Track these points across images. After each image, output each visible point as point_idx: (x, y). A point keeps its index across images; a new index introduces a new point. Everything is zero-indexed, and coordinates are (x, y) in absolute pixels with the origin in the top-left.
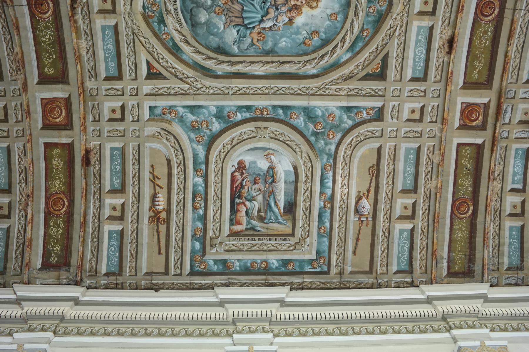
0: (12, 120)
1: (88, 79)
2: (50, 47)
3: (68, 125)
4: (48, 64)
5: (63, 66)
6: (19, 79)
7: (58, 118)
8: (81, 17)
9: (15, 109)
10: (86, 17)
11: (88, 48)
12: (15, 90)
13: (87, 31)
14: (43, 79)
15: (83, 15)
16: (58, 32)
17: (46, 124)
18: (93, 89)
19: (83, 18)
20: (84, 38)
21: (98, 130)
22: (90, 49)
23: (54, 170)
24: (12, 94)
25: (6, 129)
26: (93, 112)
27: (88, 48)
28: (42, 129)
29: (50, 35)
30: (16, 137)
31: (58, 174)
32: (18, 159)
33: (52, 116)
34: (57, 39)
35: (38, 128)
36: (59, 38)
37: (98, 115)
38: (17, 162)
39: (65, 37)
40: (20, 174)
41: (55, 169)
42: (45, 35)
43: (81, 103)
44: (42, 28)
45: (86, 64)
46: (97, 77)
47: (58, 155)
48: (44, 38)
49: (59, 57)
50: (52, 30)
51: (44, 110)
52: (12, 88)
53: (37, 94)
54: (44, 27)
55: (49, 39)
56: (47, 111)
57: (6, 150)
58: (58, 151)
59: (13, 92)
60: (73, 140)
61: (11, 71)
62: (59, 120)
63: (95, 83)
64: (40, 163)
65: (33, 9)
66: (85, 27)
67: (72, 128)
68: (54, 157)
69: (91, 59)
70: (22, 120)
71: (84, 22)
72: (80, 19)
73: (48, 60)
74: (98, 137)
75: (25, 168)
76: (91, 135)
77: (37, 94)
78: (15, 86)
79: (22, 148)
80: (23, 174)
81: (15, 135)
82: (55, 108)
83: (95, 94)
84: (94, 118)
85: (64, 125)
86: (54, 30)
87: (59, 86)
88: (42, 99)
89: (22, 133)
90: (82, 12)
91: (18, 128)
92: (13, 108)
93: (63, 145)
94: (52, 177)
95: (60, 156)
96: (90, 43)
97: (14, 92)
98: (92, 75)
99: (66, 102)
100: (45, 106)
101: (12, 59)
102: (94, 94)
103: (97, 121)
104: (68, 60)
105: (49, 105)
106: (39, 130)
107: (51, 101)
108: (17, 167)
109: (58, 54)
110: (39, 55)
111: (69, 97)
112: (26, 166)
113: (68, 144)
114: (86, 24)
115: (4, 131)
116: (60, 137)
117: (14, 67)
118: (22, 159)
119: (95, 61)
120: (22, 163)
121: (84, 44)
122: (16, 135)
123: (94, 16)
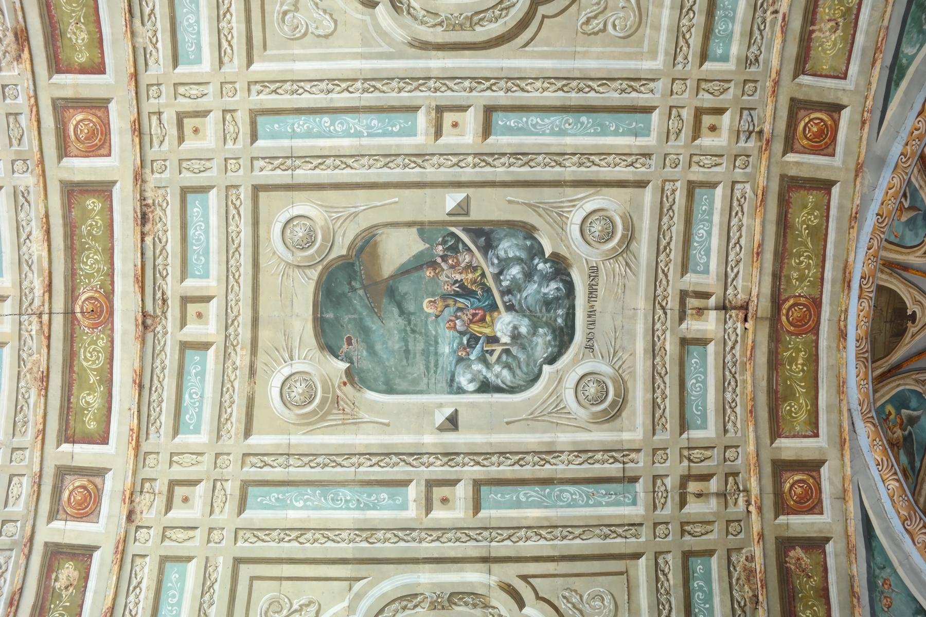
0: (169, 117)
1: (31, 189)
2: (89, 244)
3: (62, 107)
4: (95, 216)
5: (70, 212)
6: (152, 190)
7: (81, 121)
8: (36, 291)
9: (164, 137)
10: (27, 291)
11: (27, 241)
12: (160, 171)
13: (27, 268)
14: (106, 191)
15: (32, 295)
16: (72, 269)
17: (103, 109)
18: (21, 171)
19: (32, 290)
20: (35, 258)
21: (8, 99)
22: (25, 240)
23: (82, 20)
24: (167, 163)
25: (181, 100)
26: (21, 132)
27: (27, 241)
28: (108, 100)
29: (86, 264)
30: (161, 84)
31: (74, 11)
32: (157, 41)
33: (91, 125)
34: (76, 257)
35: (117, 102)
36: (72, 259)
37: (11, 126)
38: (159, 35)
39: (62, 261)
40: (153, 10)
41: (80, 21)
42: (94, 263)
43: (37, 148)
44: (98, 274)
45: (33, 214)
46: (15, 192)
47: (77, 51)
48: (96, 259)
49: (75, 227)
50: (83, 271)
51: (106, 135)
52: (166, 175)
53: (117, 164)
54: (94, 277)
55: (88, 258)
56: (102, 134)
57: (180, 59)
58: (78, 59)
59: (166, 167)
60: (50, 78)
61: (165, 205)
62: (79, 117)
63: (17, 183)
64: (112, 34)
65: (106, 304)
66: (30, 275)
67: (54, 101)
68: (84, 45)
69: (24, 223)
70: (149, 117)
71: (32, 283)
72: (37, 288)
73: (94, 223)
74: (8, 85)
75: (143, 24)
76: (19, 88)
77: (117, 164)
78: (161, 178)
79: (151, 62)
80: (147, 11)
81: (163, 88)
82: (86, 139)
83: (17, 163)
84: (16, 120)
85: (68, 108)
86: (78, 271)
87: (77, 178)
88: (109, 155)
89: (150, 92)
90: (33, 300)
91: (157, 101)
92: (167, 138)
93: (69, 71)
94: (84, 6)
95: (73, 47)
96: (24, 249)
97: (163, 167)
98: (23, 196)
99: (66, 149)
100: (105, 142)
101: (159, 225)
102: (19, 163)
103: (11, 114)
104: (60, 221)
105: (96, 145)
106: (115, 99)
107: (93, 151)
108: (159, 25)
109: (77, 232)
110: (109, 232)
111: (60, 158)
112: (141, 27)
113: (59, 71)
114: (28, 279)
115: (184, 96)
116: (76, 86)
117: (158, 212)
118: (151, 42)
119: (17, 220)
120: (150, 34)
121: (37, 248)
122: (161, 87)
123: (14, 292)
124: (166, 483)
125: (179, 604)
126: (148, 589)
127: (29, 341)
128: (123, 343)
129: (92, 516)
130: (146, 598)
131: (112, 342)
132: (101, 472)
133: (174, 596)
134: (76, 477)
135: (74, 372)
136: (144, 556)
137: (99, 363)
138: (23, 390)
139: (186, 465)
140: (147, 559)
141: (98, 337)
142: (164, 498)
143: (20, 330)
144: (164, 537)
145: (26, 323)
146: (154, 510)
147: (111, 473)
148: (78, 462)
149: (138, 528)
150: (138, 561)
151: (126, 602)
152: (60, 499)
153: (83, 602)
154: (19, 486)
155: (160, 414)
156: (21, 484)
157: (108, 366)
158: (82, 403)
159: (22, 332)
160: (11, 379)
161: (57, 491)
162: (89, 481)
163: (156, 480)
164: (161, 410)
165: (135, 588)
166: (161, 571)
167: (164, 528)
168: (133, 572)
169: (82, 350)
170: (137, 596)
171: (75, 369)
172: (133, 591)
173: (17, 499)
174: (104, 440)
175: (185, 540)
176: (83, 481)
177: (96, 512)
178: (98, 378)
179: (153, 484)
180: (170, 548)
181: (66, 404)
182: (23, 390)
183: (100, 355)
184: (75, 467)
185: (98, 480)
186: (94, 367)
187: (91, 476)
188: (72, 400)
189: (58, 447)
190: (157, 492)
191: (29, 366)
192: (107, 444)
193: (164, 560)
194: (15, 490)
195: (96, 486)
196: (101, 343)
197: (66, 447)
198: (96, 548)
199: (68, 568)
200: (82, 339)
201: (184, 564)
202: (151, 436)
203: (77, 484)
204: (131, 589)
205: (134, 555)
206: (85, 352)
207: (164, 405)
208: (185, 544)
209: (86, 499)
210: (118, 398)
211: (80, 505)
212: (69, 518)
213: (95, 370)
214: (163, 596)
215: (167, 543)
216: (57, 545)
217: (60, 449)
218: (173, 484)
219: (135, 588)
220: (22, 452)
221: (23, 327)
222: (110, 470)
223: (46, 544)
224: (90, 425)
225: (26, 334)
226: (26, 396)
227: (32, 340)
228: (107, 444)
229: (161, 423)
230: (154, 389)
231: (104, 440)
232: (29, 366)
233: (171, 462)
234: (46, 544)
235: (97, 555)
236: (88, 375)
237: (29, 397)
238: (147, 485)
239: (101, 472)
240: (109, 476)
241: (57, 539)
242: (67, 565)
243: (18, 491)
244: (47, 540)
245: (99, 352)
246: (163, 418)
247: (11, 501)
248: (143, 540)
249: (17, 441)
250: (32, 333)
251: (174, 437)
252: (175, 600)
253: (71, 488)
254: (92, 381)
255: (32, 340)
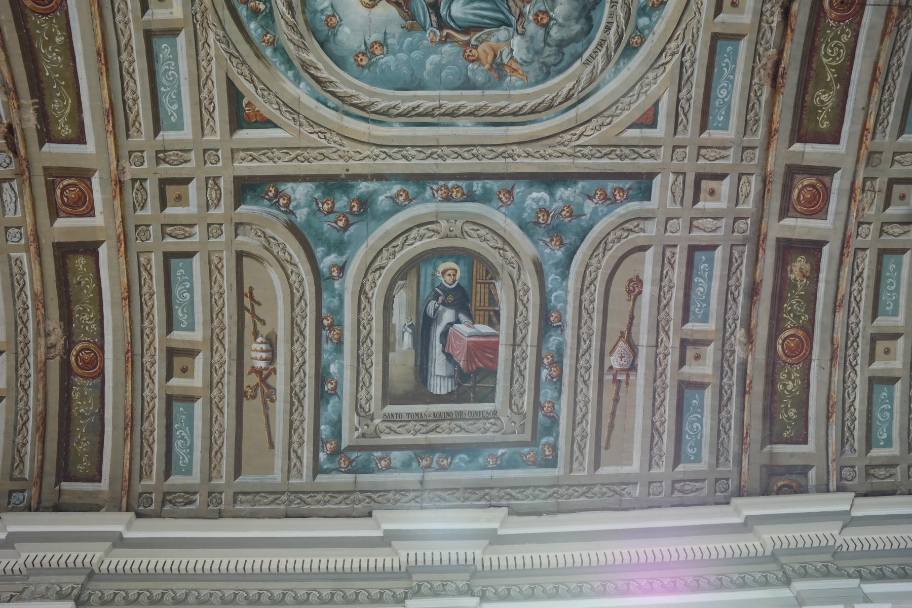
124: (886, 180)
125: (897, 290)
126: (868, 278)
127: (768, 34)
128: (869, 38)
129: (820, 213)
130: (868, 286)
131: (856, 37)
132: (830, 171)
133: (892, 284)
134: (805, 176)
135: (812, 69)
136: (865, 249)
137: (839, 60)
138: (756, 87)
139: (906, 163)
140: (868, 252)
141: (843, 32)
142: (883, 196)
143: (761, 21)
144: (882, 232)
145: (768, 14)
146: (874, 207)
147: (840, 172)
148: (808, 161)
149: (860, 224)
150: (860, 254)
151: (850, 290)
152: (790, 197)
153: (816, 291)
154: (747, 184)
155: (889, 113)
156: (749, 182)
157: (849, 63)
158: (816, 101)
159: (762, 24)
160: (744, 75)
161: (787, 189)
162: (817, 179)
163: (876, 178)
164: (890, 110)
165: (858, 278)
166: (880, 263)
167: (882, 223)
168: (855, 264)
169: (823, 46)
170: (860, 285)
171: (814, 66)
172: (856, 280)
173: (746, 197)
174: (836, 141)
175: (900, 234)
176: (813, 180)
177: (824, 210)
178: (836, 75)
179: (874, 183)
180: (888, 241)
181: (800, 103)
182: (756, 87)
183: (842, 51)
184: (805, 167)
185: (826, 179)
186: (833, 64)
187: (821, 175)
188: (806, 99)
189: (789, 147)
190: (877, 189)
191: (764, 61)
192: (838, 143)
193: (882, 252)
194: (744, 189)
195: (824, 185)
196: (845, 38)
197: (797, 147)
198: (825, 243)
199: (800, 261)
200: (825, 33)
201: (899, 256)
202: (877, 136)
203: (806, 183)
204: (854, 278)
205: (856, 249)
206: (825, 48)
207: (894, 104)
208: (901, 238)
209: (815, 197)
210: (853, 97)
211: (810, 202)
212: (799, 215)
213: (833, 67)
214: (882, 284)
215: (885, 237)
216: (788, 240)
217: (792, 149)
218: (892, 182)
219: (858, 278)
220: (752, 151)
221: (764, 18)
222: (840, 169)
223: (778, 240)
224: (823, 125)
225: (766, 26)
226: (758, 94)
227: (772, 33)
228: (838, 143)
229: (888, 123)
230: (887, 88)
231: (836, 141)
232: (763, 62)
233: (893, 162)
234: (778, 240)
235: (826, 249)
236: (826, 72)
237: (761, 95)
238: (868, 183)
239: (830, 171)
240: (837, 175)
241: (788, 235)
242: (799, 259)
243: (746, 189)
244: (780, 236)
245: (840, 48)
246: (891, 118)
247: (741, 199)
248: (864, 235)
249: (747, 140)
250: (772, 25)
251: (899, 137)
252: (893, 287)
253: (800, 186)
254: (828, 80)
255: (772, 33)
